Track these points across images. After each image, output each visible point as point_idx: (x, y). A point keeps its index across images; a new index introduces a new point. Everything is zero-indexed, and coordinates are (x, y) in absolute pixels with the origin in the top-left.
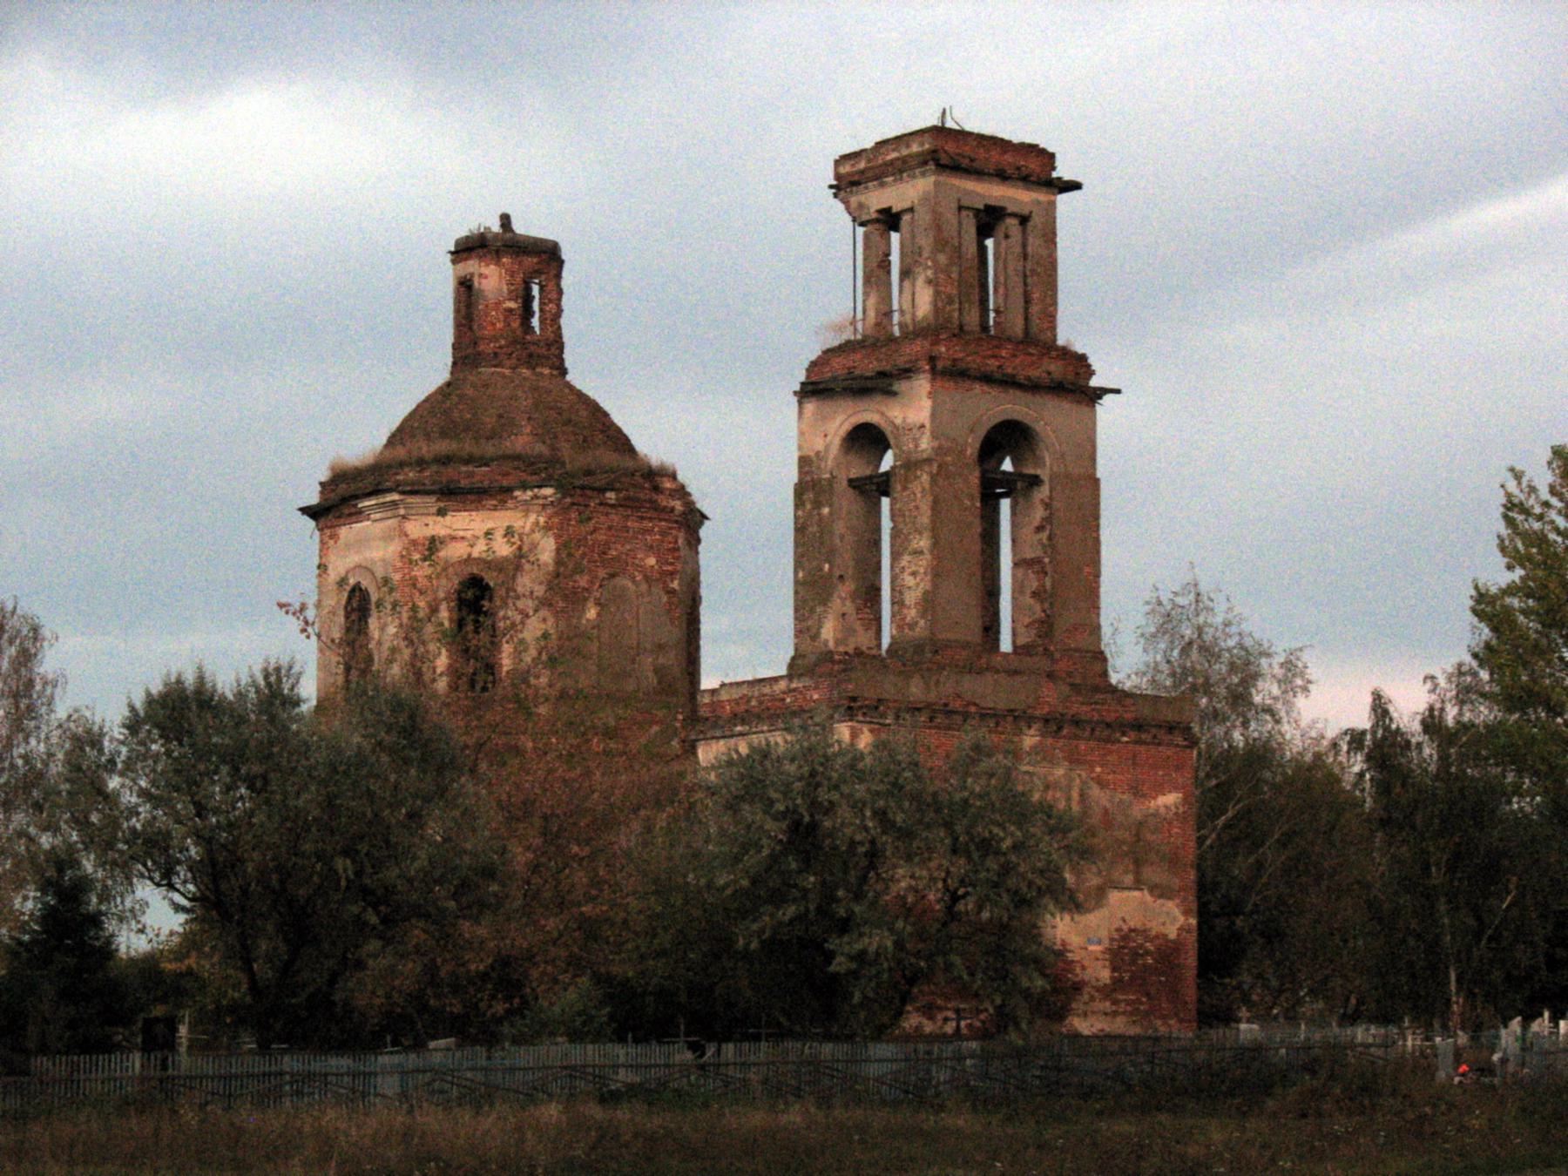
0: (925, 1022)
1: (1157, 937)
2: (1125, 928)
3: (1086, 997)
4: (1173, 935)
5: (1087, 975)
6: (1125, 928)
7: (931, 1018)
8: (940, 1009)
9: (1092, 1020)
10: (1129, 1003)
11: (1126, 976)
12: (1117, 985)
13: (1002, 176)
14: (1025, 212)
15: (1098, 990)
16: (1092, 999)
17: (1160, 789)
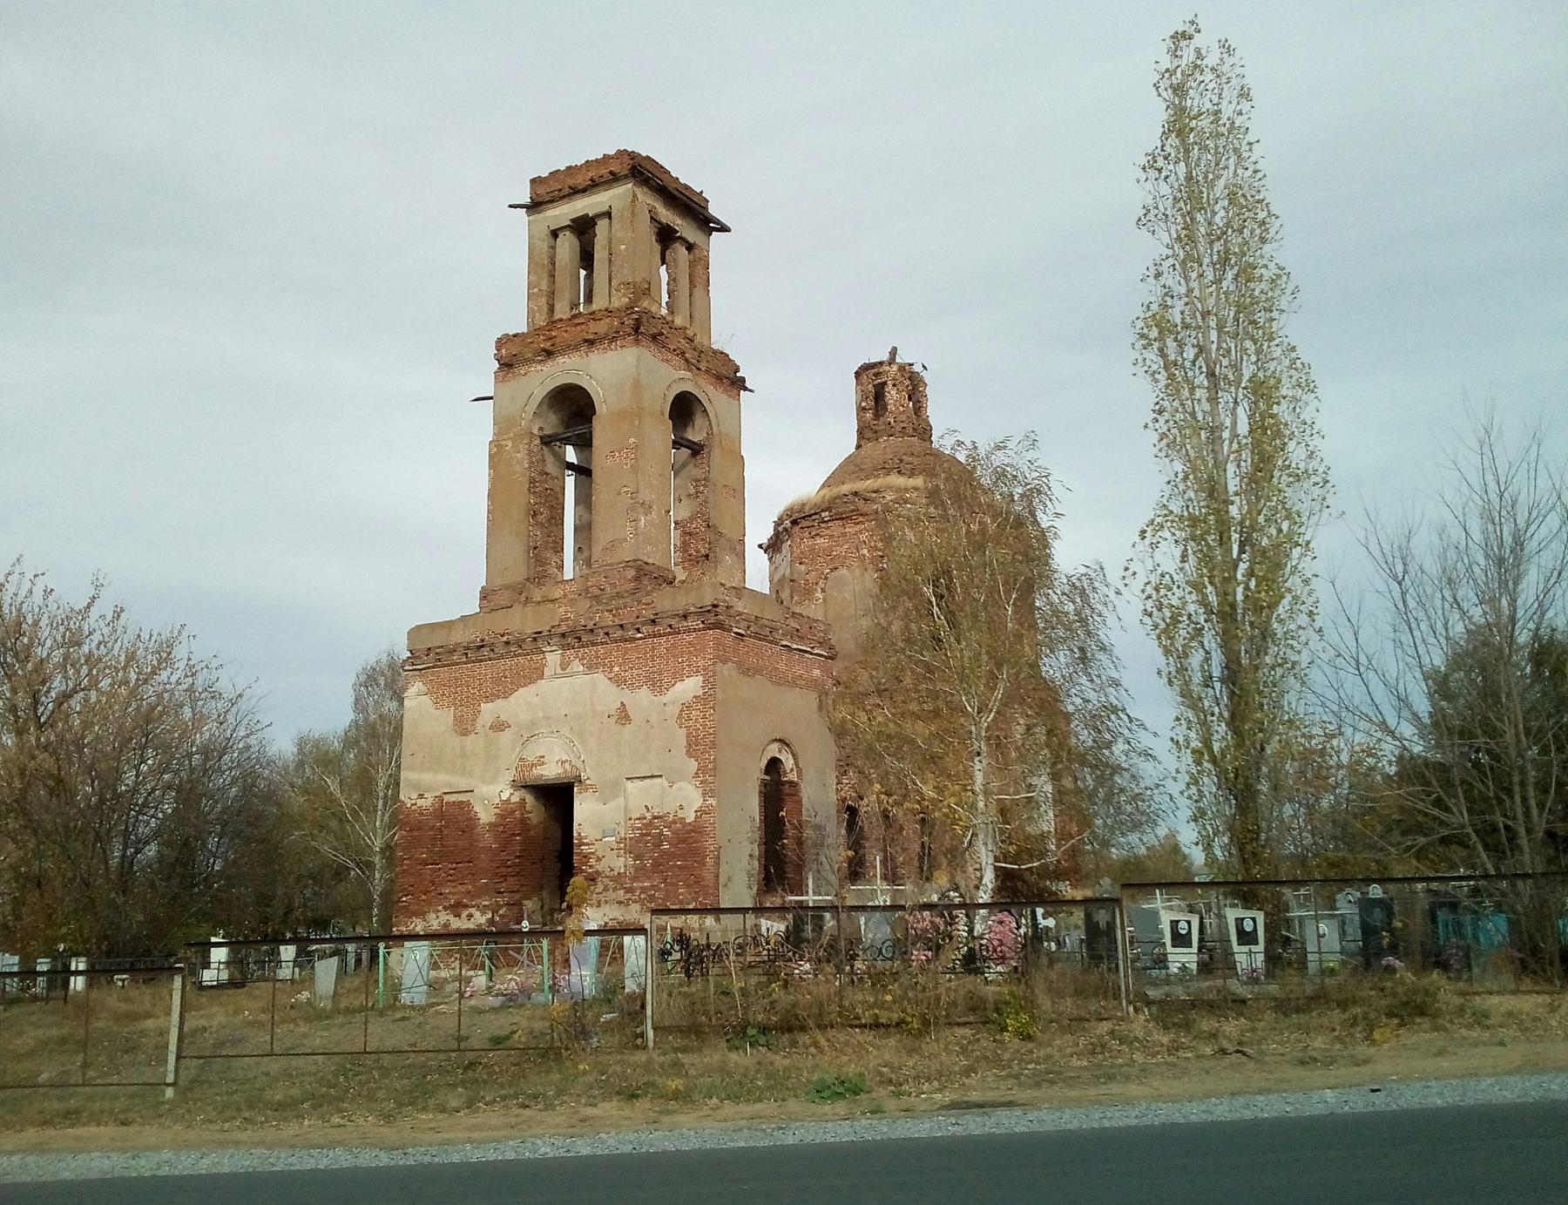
0: (451, 918)
1: (674, 822)
2: (648, 815)
3: (600, 888)
4: (691, 818)
5: (599, 868)
6: (648, 815)
7: (458, 916)
8: (466, 906)
9: (606, 909)
10: (643, 890)
11: (649, 863)
12: (640, 873)
13: (576, 192)
14: (606, 209)
15: (612, 879)
16: (606, 889)
17: (678, 676)
